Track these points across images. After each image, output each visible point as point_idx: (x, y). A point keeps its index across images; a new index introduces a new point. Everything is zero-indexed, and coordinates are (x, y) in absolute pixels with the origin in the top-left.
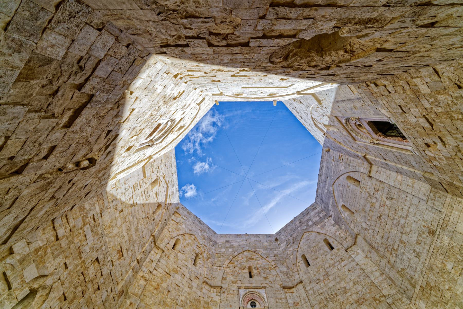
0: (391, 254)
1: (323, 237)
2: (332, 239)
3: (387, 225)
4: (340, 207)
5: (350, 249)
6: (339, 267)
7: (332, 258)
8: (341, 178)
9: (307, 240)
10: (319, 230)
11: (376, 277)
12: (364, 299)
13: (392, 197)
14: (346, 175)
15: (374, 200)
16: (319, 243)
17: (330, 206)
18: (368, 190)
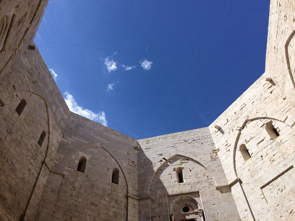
0: (64, 215)
1: (46, 130)
2: (47, 142)
3: (91, 212)
4: (81, 154)
5: (46, 167)
6: (29, 158)
7: (34, 147)
8: (113, 160)
9: (39, 106)
10: (51, 122)
11: (34, 200)
12: (15, 193)
13: (118, 217)
14: (118, 167)
15: (107, 199)
16: (41, 125)
17: (77, 138)
18: (114, 193)
